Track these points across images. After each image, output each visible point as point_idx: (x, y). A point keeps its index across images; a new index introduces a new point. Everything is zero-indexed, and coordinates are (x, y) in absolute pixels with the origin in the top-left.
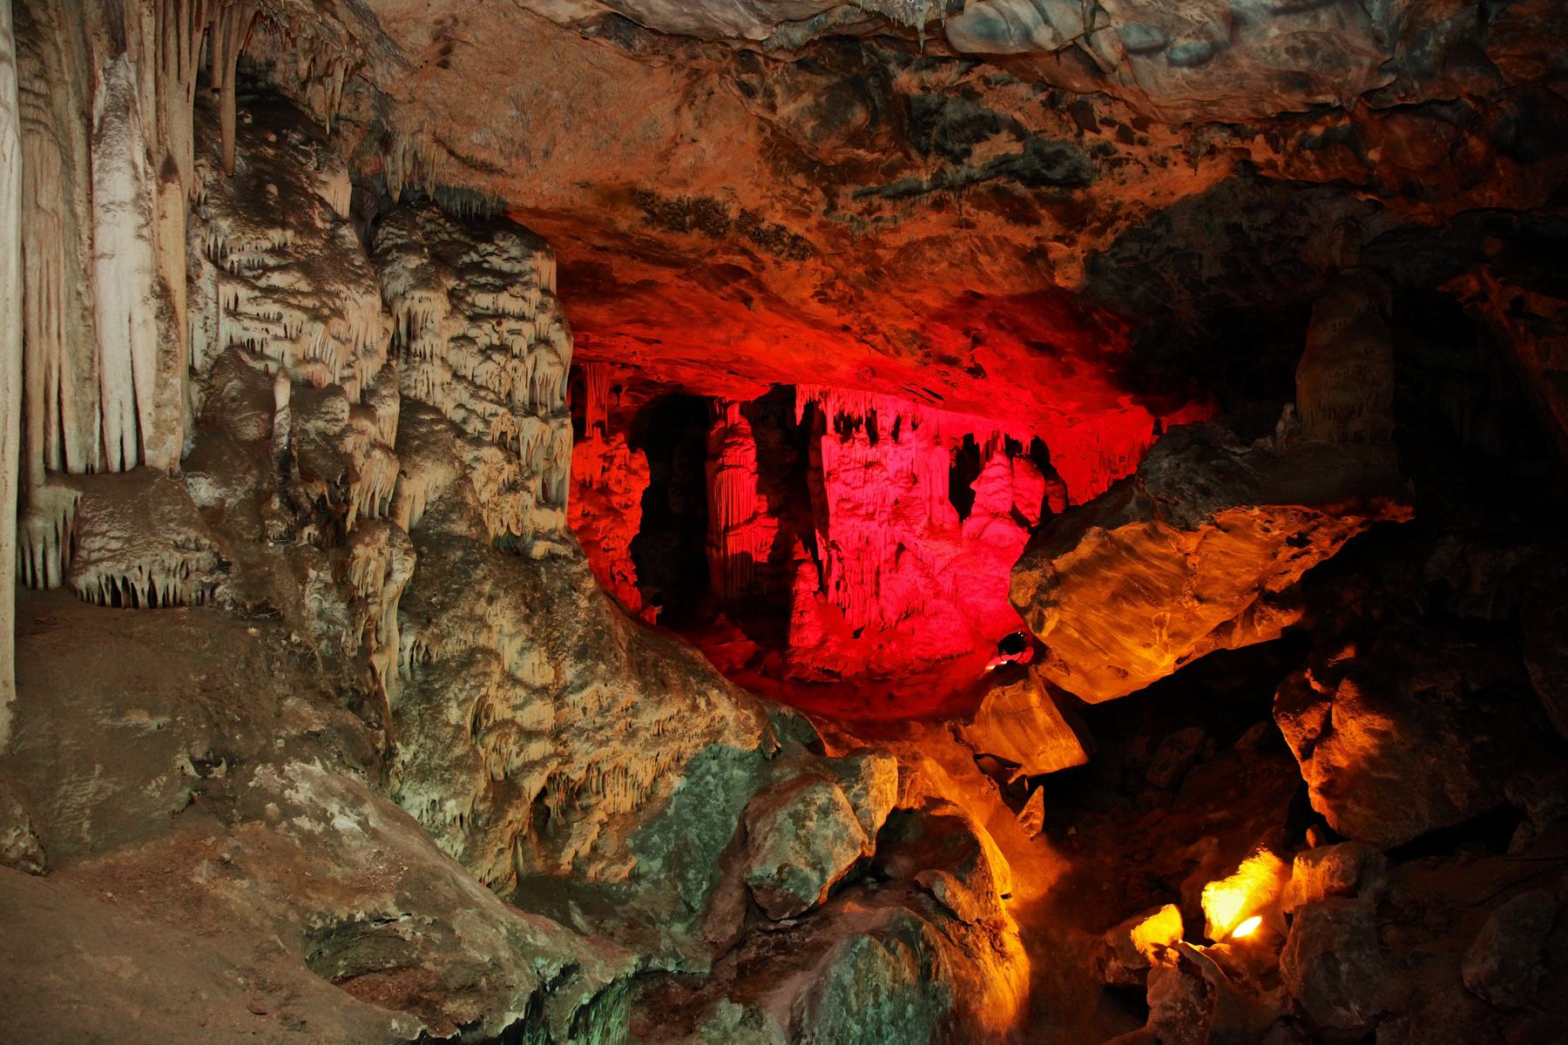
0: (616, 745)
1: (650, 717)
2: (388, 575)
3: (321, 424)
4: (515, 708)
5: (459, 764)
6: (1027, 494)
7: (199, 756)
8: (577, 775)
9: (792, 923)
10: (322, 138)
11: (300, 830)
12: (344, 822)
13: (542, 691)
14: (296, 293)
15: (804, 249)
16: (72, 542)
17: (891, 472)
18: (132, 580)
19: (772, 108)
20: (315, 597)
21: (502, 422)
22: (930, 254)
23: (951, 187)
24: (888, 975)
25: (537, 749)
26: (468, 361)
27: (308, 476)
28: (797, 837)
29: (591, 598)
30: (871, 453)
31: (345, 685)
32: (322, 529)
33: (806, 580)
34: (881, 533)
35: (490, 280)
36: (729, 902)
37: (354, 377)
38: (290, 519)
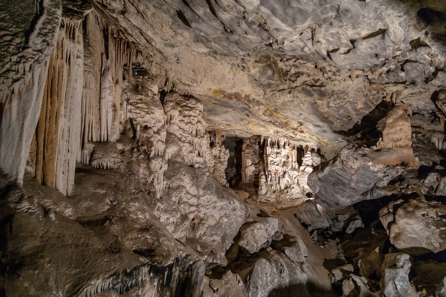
0: (211, 209)
1: (219, 204)
2: (161, 168)
3: (147, 135)
4: (189, 199)
5: (174, 210)
6: (316, 161)
7: (111, 199)
8: (202, 215)
9: (249, 256)
10: (153, 78)
11: (130, 217)
12: (140, 216)
13: (195, 196)
14: (143, 108)
15: (260, 104)
16: (92, 155)
17: (283, 155)
18: (103, 163)
19: (249, 71)
20: (142, 171)
21: (190, 138)
22: (289, 104)
23: (292, 88)
24: (270, 270)
25: (193, 209)
26: (183, 125)
27: (142, 145)
28: (252, 235)
29: (207, 177)
30: (278, 151)
31: (147, 189)
32: (145, 156)
33: (263, 179)
34: (280, 169)
35: (188, 108)
36: (235, 250)
37: (156, 126)
38: (138, 154)
